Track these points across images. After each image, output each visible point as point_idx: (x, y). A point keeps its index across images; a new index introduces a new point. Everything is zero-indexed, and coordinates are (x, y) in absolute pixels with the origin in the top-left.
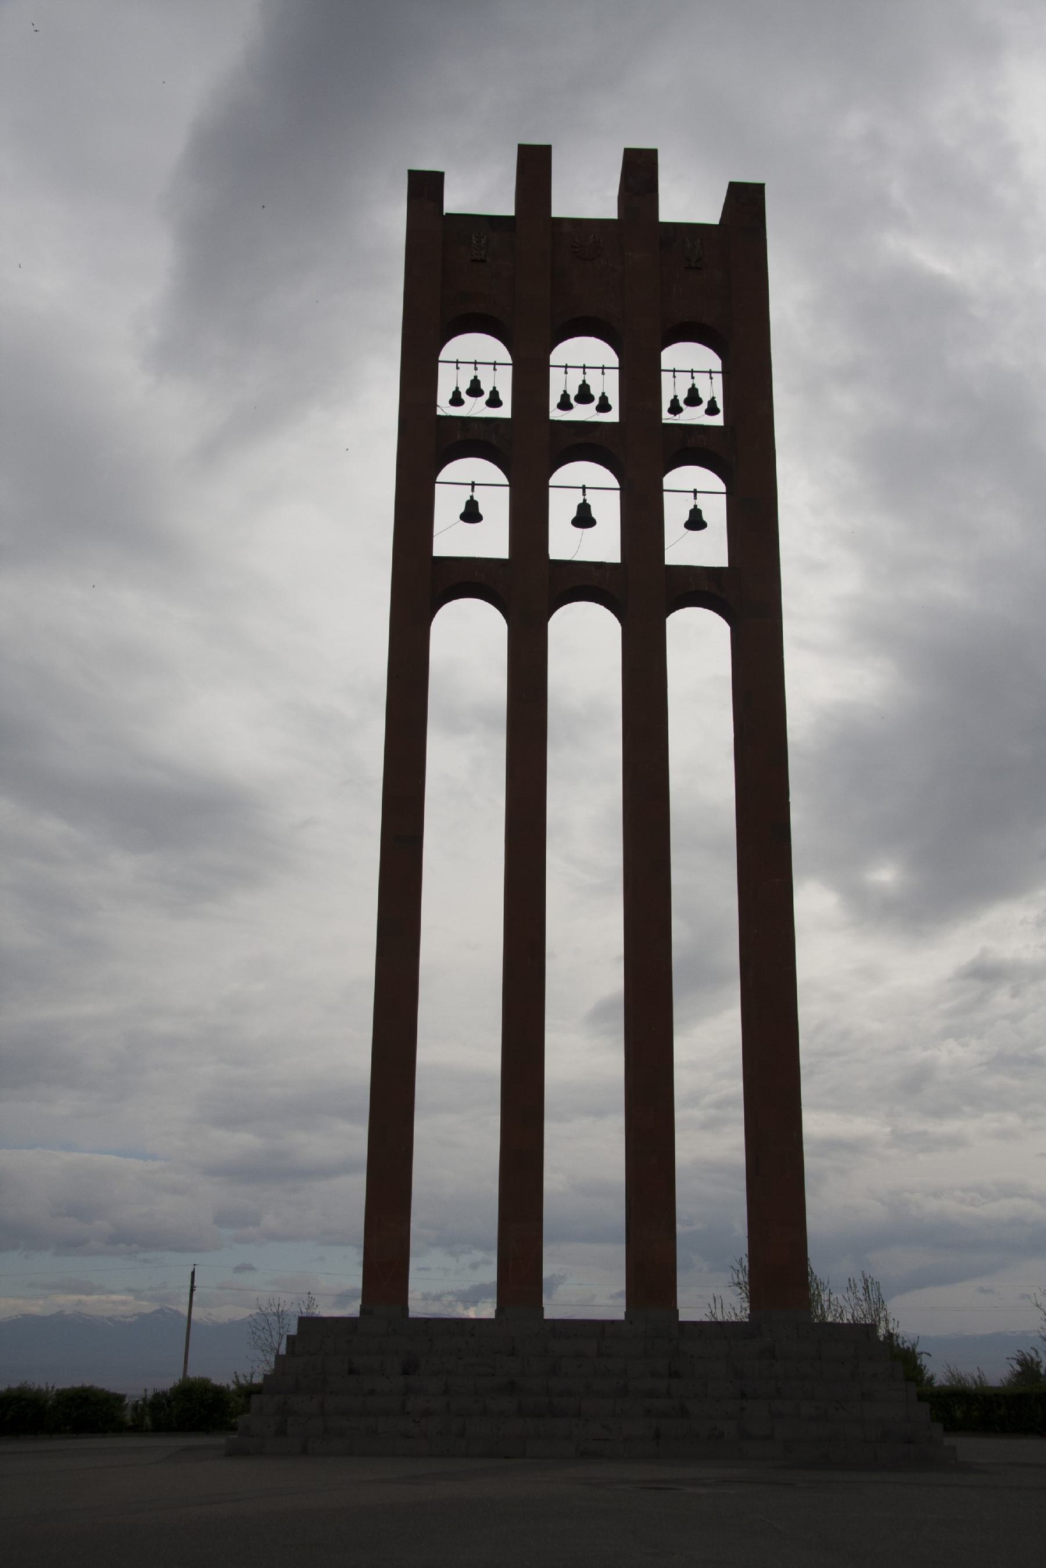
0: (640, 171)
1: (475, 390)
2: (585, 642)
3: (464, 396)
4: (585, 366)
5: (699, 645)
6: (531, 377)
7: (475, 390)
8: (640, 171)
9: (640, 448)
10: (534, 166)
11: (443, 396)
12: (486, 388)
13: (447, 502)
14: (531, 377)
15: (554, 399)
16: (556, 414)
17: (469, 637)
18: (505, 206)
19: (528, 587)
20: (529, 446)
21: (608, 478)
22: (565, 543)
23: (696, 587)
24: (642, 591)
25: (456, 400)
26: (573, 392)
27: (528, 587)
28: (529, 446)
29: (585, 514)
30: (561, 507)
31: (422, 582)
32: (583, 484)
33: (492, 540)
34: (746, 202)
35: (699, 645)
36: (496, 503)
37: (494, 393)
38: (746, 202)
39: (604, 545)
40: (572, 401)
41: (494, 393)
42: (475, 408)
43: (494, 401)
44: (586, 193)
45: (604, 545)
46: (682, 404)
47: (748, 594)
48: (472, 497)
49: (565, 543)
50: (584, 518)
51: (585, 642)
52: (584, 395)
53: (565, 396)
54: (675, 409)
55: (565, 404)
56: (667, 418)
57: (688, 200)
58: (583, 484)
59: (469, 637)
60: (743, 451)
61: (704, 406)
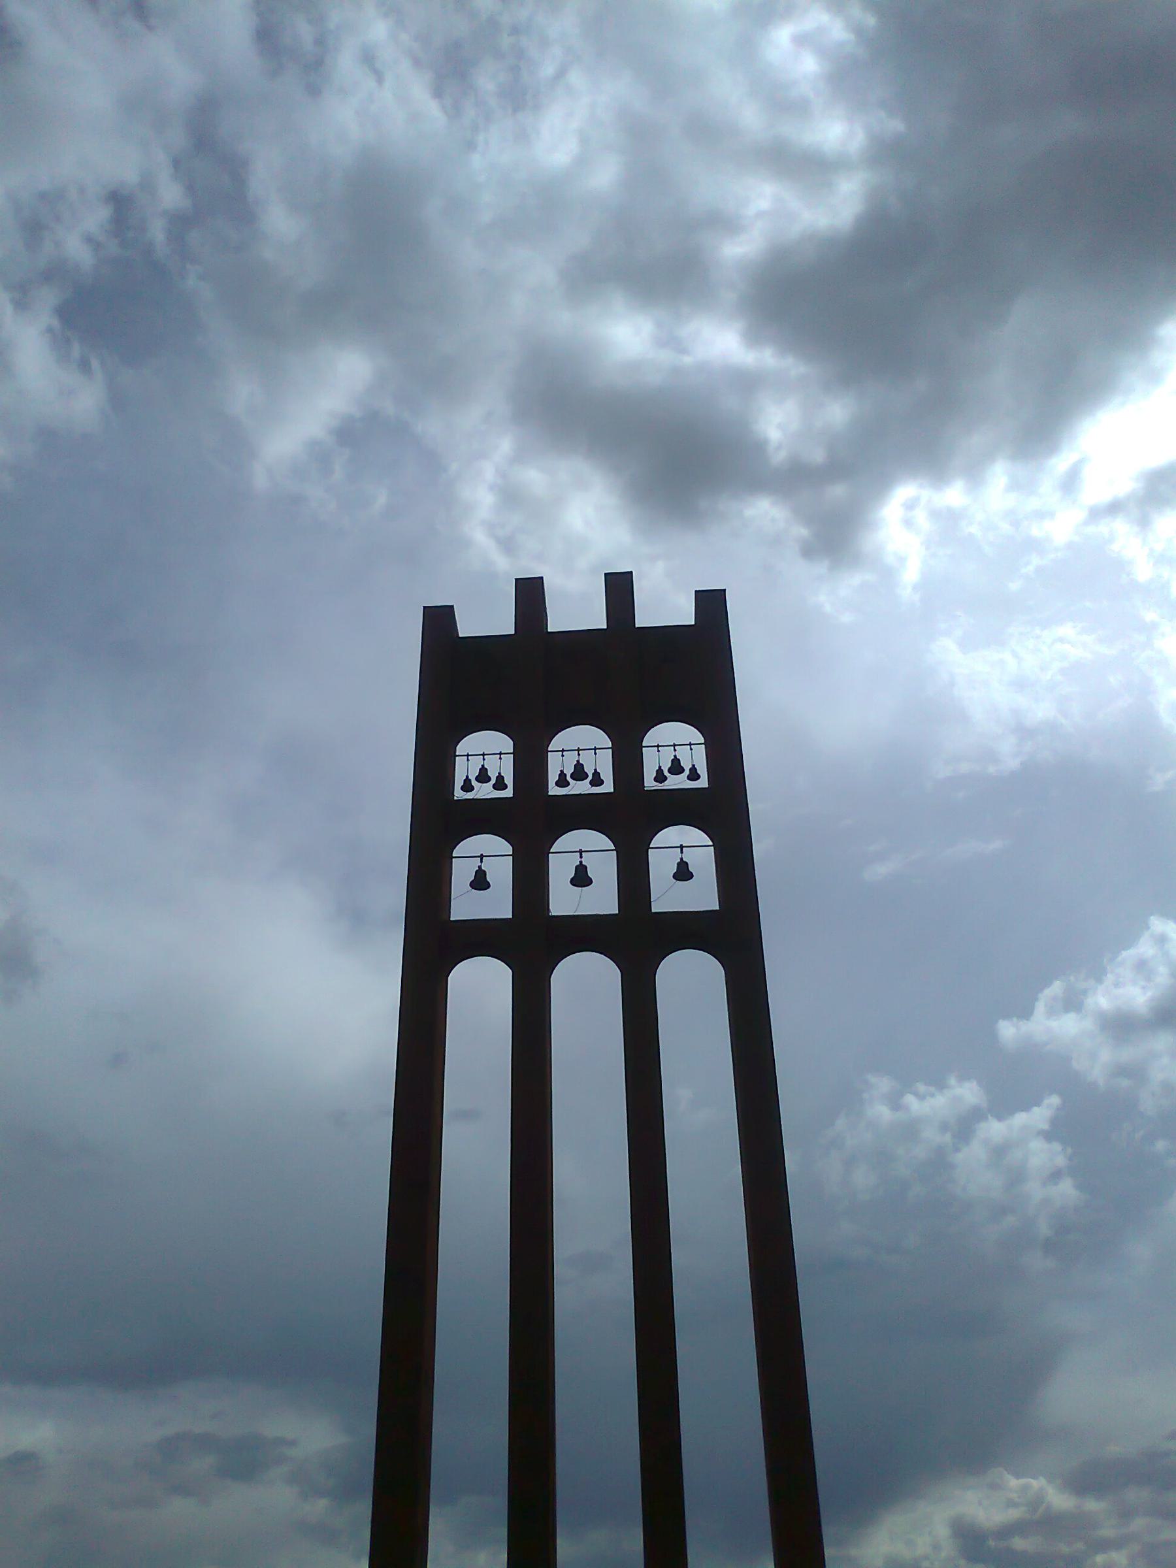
0: (619, 588)
1: (483, 777)
2: (585, 987)
3: (474, 783)
4: (581, 752)
5: (691, 984)
6: (531, 762)
7: (483, 777)
8: (619, 588)
9: (632, 815)
10: (530, 593)
11: (459, 782)
12: (493, 775)
13: (461, 872)
14: (531, 762)
15: (553, 777)
16: (554, 790)
17: (480, 990)
18: (506, 626)
19: (533, 942)
20: (531, 820)
21: (604, 842)
22: (564, 900)
23: (686, 931)
24: (637, 939)
25: (468, 786)
26: (569, 771)
27: (533, 942)
28: (531, 820)
29: (583, 875)
30: (560, 868)
31: (433, 947)
32: (586, 848)
33: (497, 904)
34: (712, 604)
35: (691, 984)
36: (501, 872)
37: (500, 778)
38: (712, 604)
39: (602, 899)
40: (569, 778)
41: (500, 778)
42: (485, 791)
43: (500, 784)
44: (577, 609)
45: (602, 899)
46: (666, 773)
47: (732, 933)
48: (480, 867)
49: (564, 900)
50: (581, 878)
51: (585, 987)
52: (579, 773)
53: (562, 775)
54: (660, 777)
55: (562, 782)
56: (650, 783)
57: (664, 605)
58: (586, 848)
59: (480, 990)
60: (721, 807)
61: (687, 772)
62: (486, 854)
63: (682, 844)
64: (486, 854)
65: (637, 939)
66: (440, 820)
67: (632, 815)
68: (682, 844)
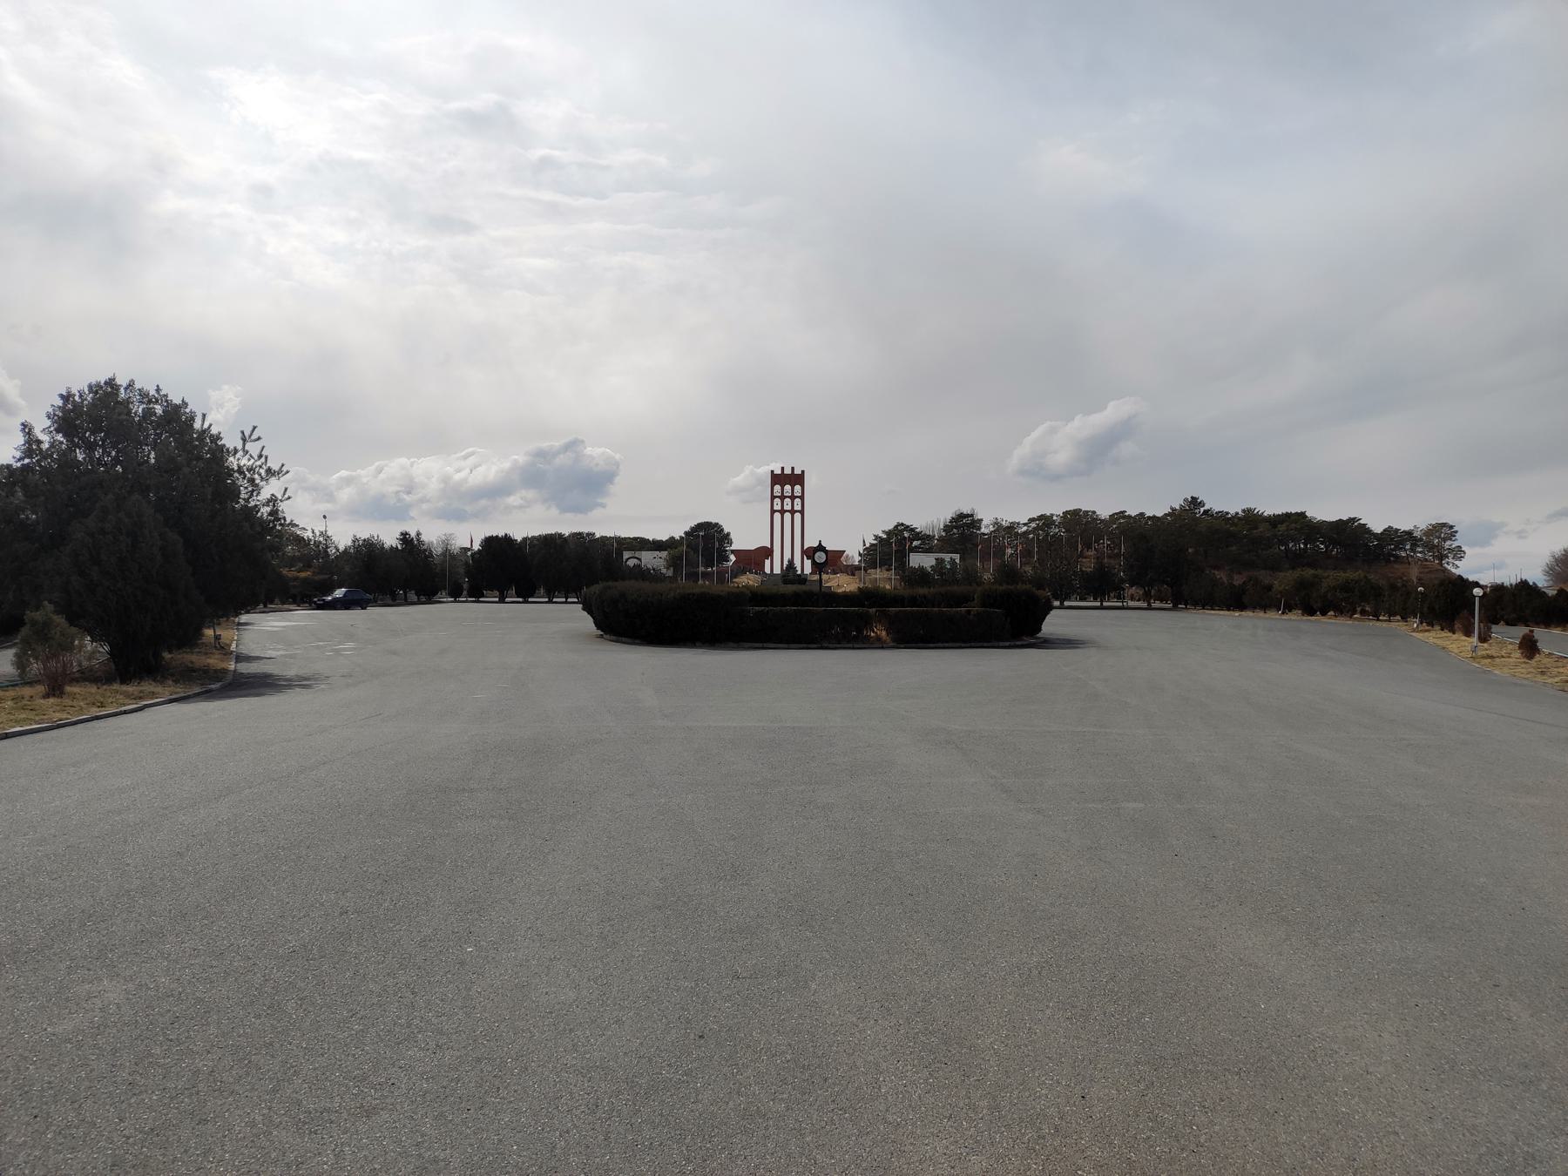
2: (788, 516)
4: (788, 488)
5: (798, 516)
9: (793, 498)
17: (777, 516)
19: (782, 512)
20: (782, 498)
24: (793, 512)
27: (782, 512)
28: (782, 498)
31: (773, 512)
32: (788, 501)
35: (798, 516)
44: (788, 471)
51: (788, 516)
57: (797, 472)
58: (788, 501)
59: (777, 516)
60: (802, 498)
62: (777, 501)
63: (798, 501)
64: (777, 501)
65: (793, 512)
66: (773, 497)
67: (793, 498)
68: (798, 501)
